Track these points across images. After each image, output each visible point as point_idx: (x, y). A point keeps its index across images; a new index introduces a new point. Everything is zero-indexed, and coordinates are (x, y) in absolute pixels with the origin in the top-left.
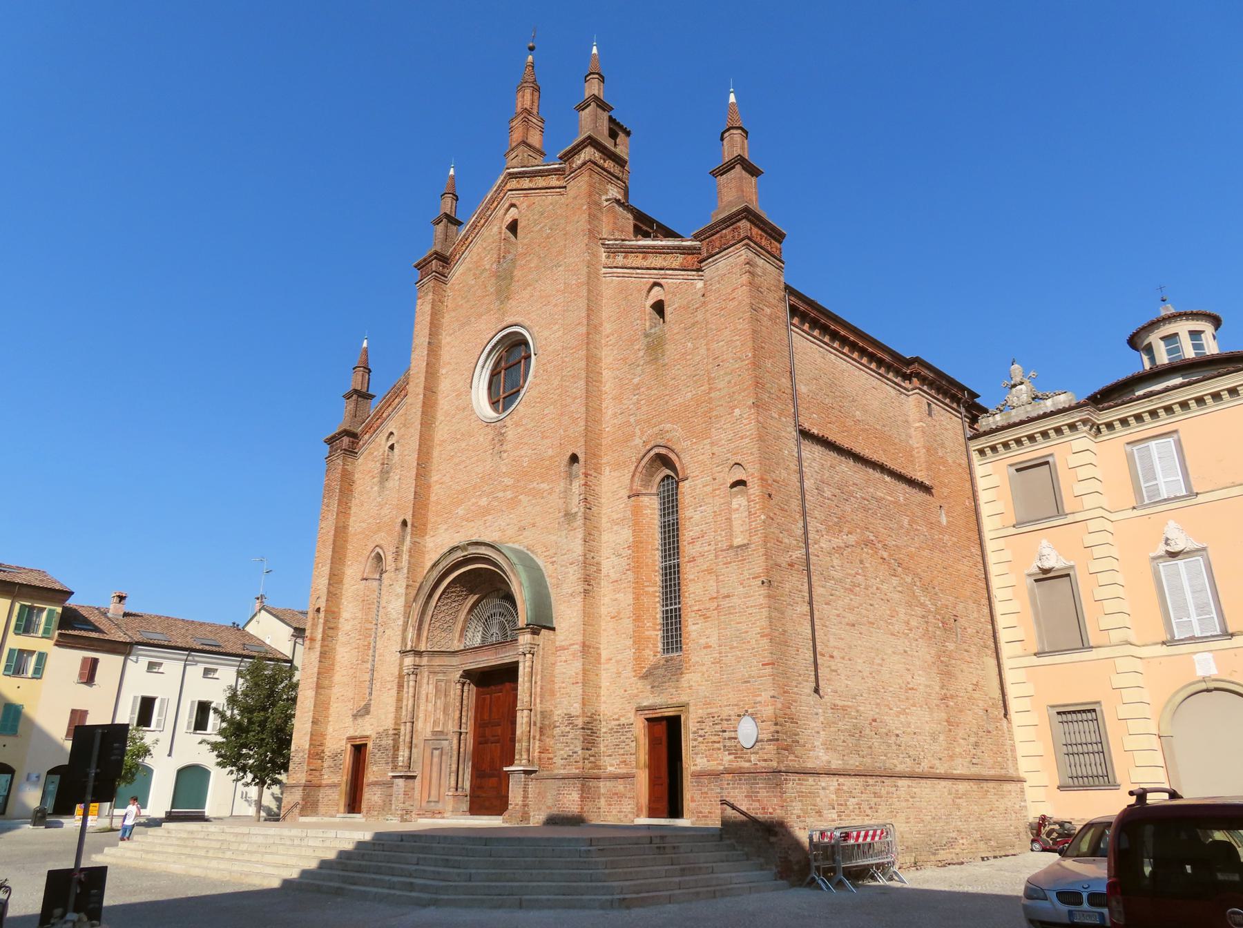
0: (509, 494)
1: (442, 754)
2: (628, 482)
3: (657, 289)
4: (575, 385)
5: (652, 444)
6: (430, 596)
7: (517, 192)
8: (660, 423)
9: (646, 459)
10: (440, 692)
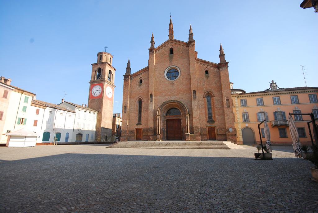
0: (176, 93)
9: (207, 93)
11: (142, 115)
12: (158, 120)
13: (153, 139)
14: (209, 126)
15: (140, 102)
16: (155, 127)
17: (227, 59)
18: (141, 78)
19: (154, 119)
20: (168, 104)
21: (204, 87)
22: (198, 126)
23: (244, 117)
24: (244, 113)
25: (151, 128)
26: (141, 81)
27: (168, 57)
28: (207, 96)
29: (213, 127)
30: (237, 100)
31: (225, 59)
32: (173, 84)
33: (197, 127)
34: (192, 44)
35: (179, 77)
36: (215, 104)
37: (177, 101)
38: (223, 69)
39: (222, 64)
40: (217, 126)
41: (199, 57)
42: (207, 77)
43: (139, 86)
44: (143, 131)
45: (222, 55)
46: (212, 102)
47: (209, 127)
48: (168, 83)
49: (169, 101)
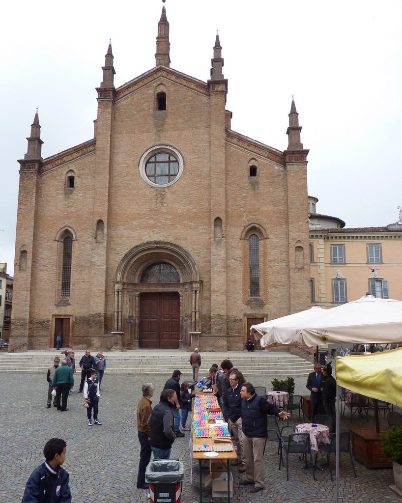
1: (131, 325)
2: (240, 233)
3: (253, 161)
4: (219, 189)
5: (252, 222)
6: (131, 260)
7: (169, 80)
8: (257, 215)
9: (249, 227)
10: (131, 301)
11: (72, 280)
12: (116, 293)
13: (101, 346)
14: (250, 315)
15: (67, 238)
16: (109, 313)
17: (306, 140)
18: (71, 171)
19: (106, 291)
20: (146, 252)
21: (244, 211)
22: (223, 313)
23: (337, 289)
24: (338, 279)
25: (99, 315)
26: (71, 181)
27: (151, 117)
28: (250, 235)
29: (260, 317)
30: (322, 246)
31: (301, 142)
32: (161, 195)
33: (220, 315)
34: (221, 88)
36: (269, 258)
37: (171, 244)
38: (295, 166)
39: (293, 153)
40: (269, 314)
41: (236, 126)
42: (254, 185)
43: (66, 194)
44: (73, 322)
45: (294, 130)
46: (261, 253)
47: (250, 317)
48: (148, 193)
49: (150, 243)
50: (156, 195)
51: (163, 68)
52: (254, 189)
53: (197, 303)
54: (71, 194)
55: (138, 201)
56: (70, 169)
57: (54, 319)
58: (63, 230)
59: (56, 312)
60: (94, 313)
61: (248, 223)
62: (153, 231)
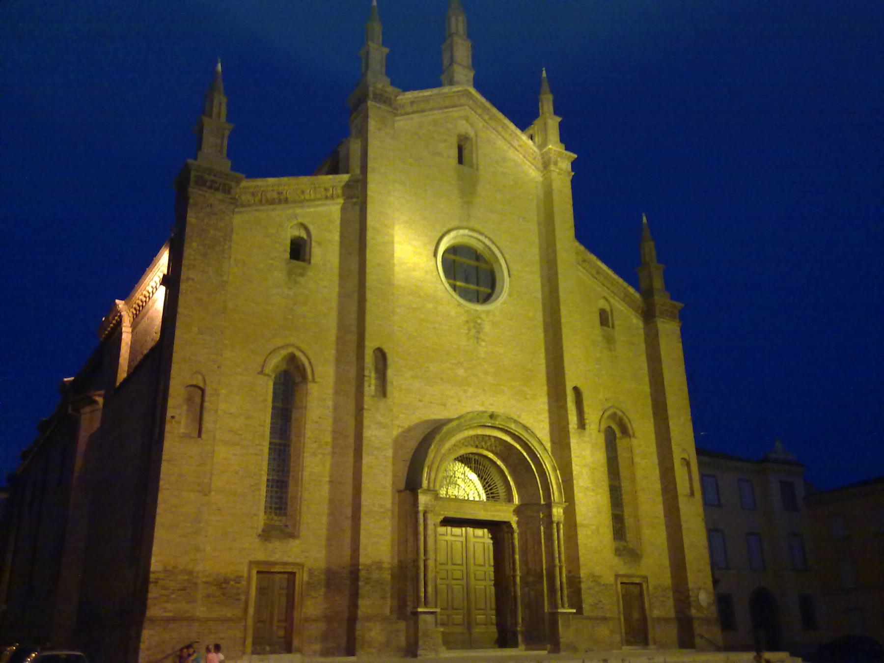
25: (379, 565)
29: (637, 581)
35: (505, 303)
36: (639, 473)
47: (625, 580)
48: (453, 313)
50: (467, 322)
51: (470, 93)
52: (610, 350)
53: (562, 548)
54: (302, 275)
55: (437, 326)
56: (300, 220)
57: (254, 572)
58: (284, 353)
59: (260, 556)
60: (369, 562)
61: (607, 405)
62: (465, 391)
